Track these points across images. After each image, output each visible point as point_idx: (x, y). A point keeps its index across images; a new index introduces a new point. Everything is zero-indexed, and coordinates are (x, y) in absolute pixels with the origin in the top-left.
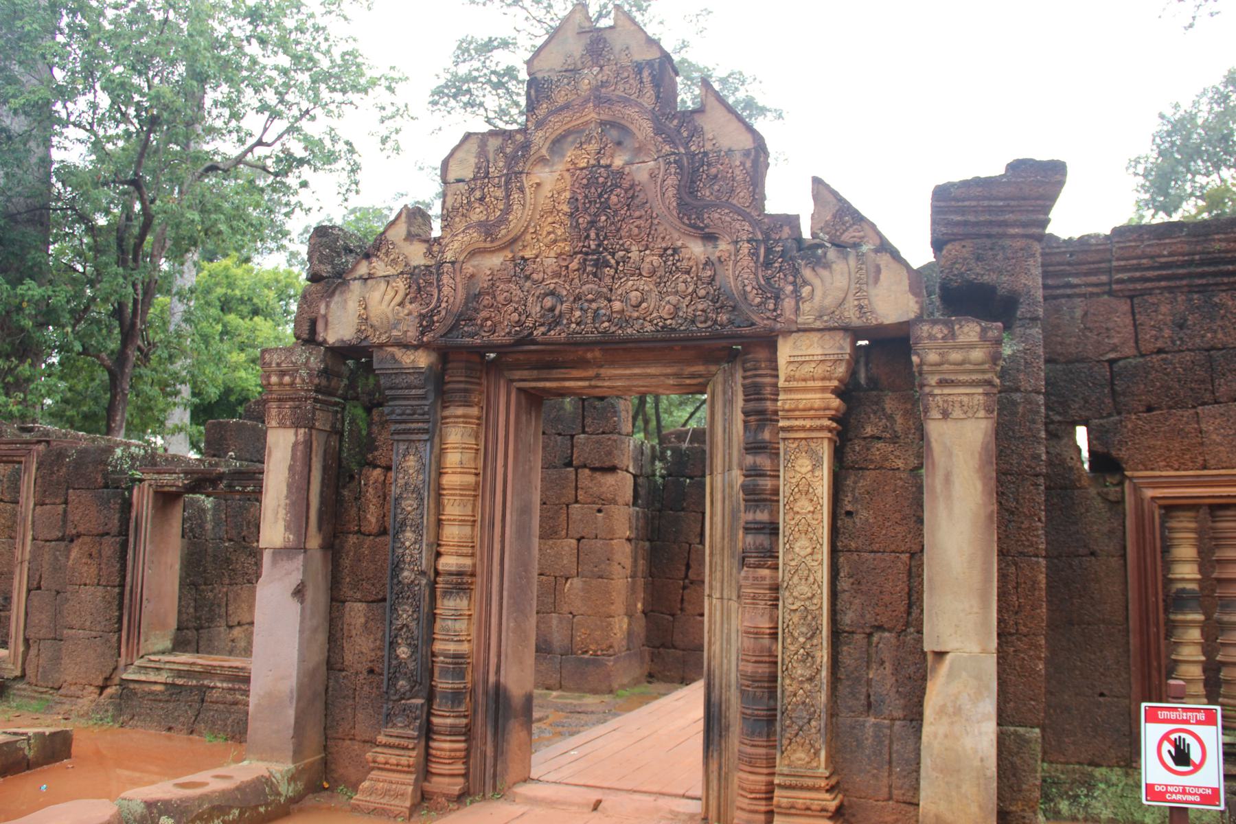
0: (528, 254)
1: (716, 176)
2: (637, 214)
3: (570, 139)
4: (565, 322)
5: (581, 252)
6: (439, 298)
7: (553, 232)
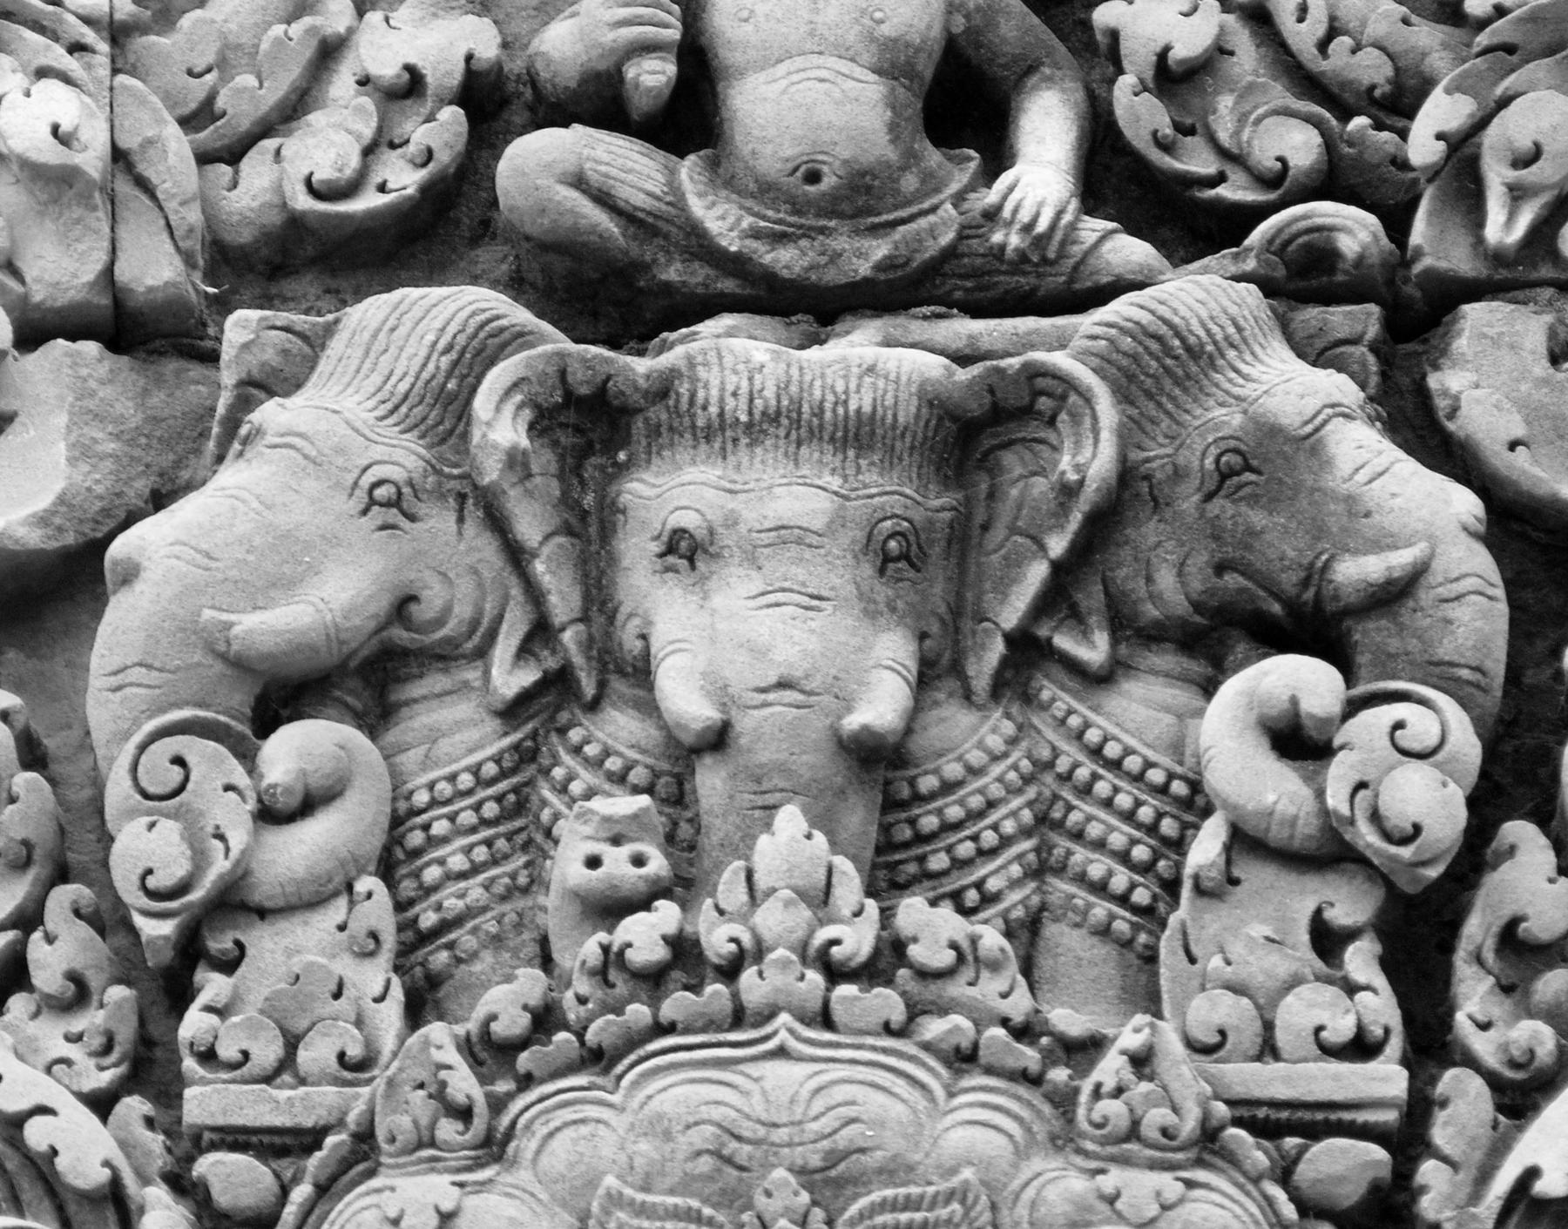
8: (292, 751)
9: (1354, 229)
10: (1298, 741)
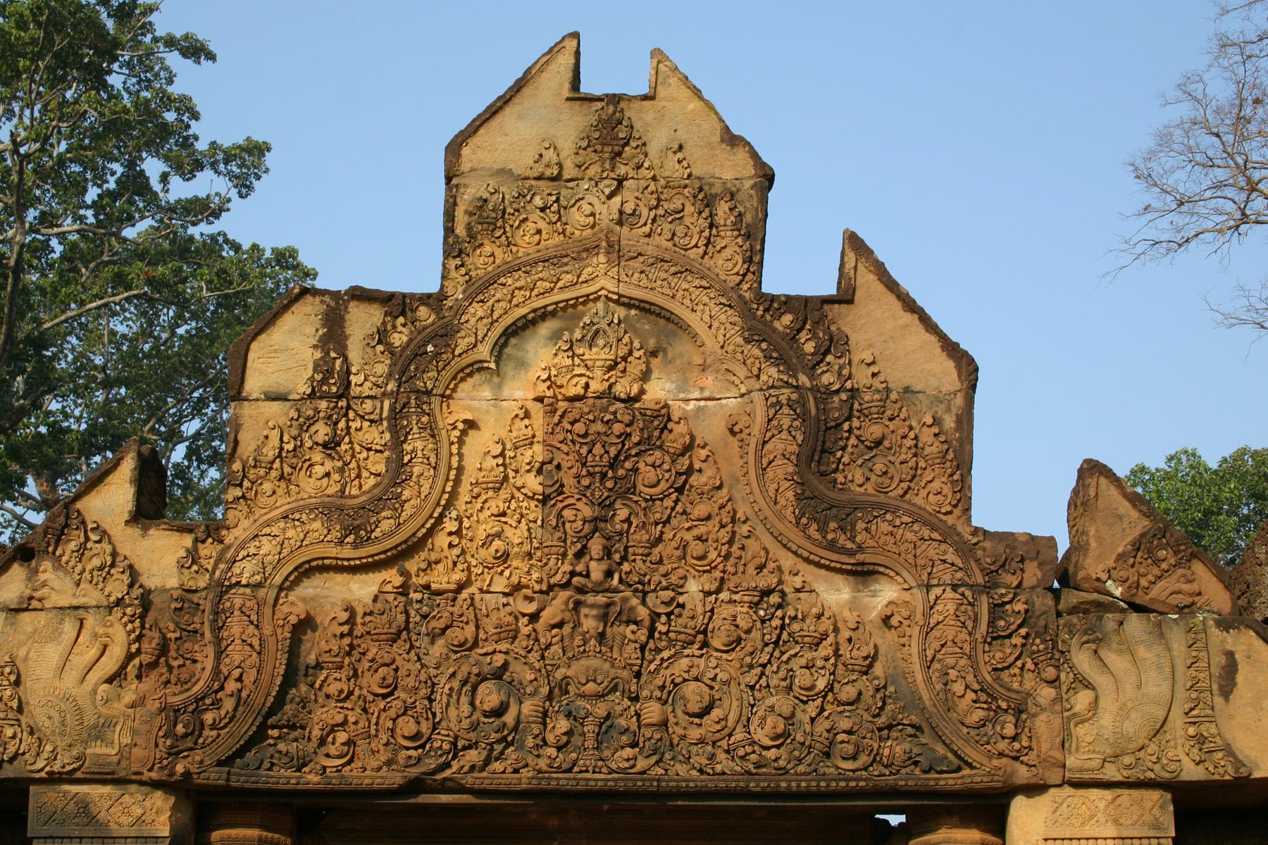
0: (441, 578)
1: (878, 443)
2: (700, 510)
3: (545, 328)
4: (530, 742)
5: (565, 586)
6: (216, 671)
7: (498, 535)
8: (555, 631)
9: (640, 587)
10: (633, 632)
